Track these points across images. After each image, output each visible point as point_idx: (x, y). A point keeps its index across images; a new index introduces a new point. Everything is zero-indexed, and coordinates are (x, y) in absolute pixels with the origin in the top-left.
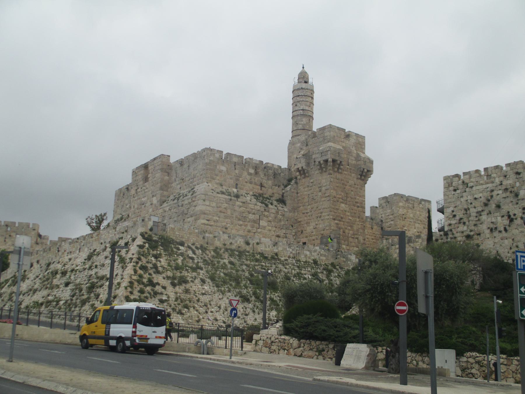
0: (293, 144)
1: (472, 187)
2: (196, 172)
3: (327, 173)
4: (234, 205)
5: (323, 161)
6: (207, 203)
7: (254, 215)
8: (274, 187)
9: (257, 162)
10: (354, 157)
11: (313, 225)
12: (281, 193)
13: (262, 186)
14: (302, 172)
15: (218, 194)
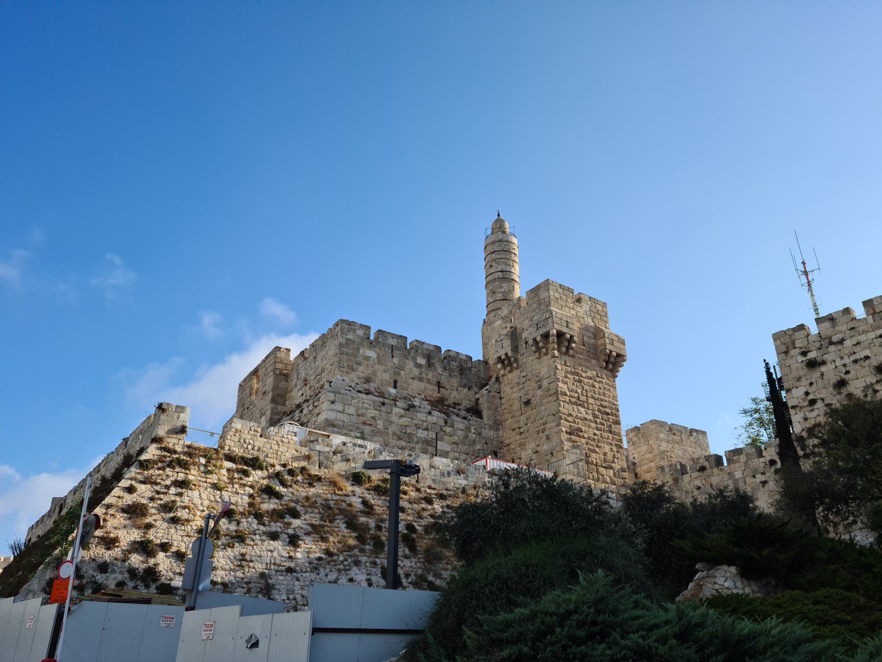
0: (490, 324)
1: (841, 342)
2: (325, 362)
3: (549, 355)
4: (389, 413)
5: (541, 336)
6: (339, 406)
7: (426, 432)
8: (460, 389)
9: (431, 348)
10: (593, 334)
11: (531, 446)
12: (474, 399)
13: (439, 385)
14: (506, 362)
15: (359, 394)
